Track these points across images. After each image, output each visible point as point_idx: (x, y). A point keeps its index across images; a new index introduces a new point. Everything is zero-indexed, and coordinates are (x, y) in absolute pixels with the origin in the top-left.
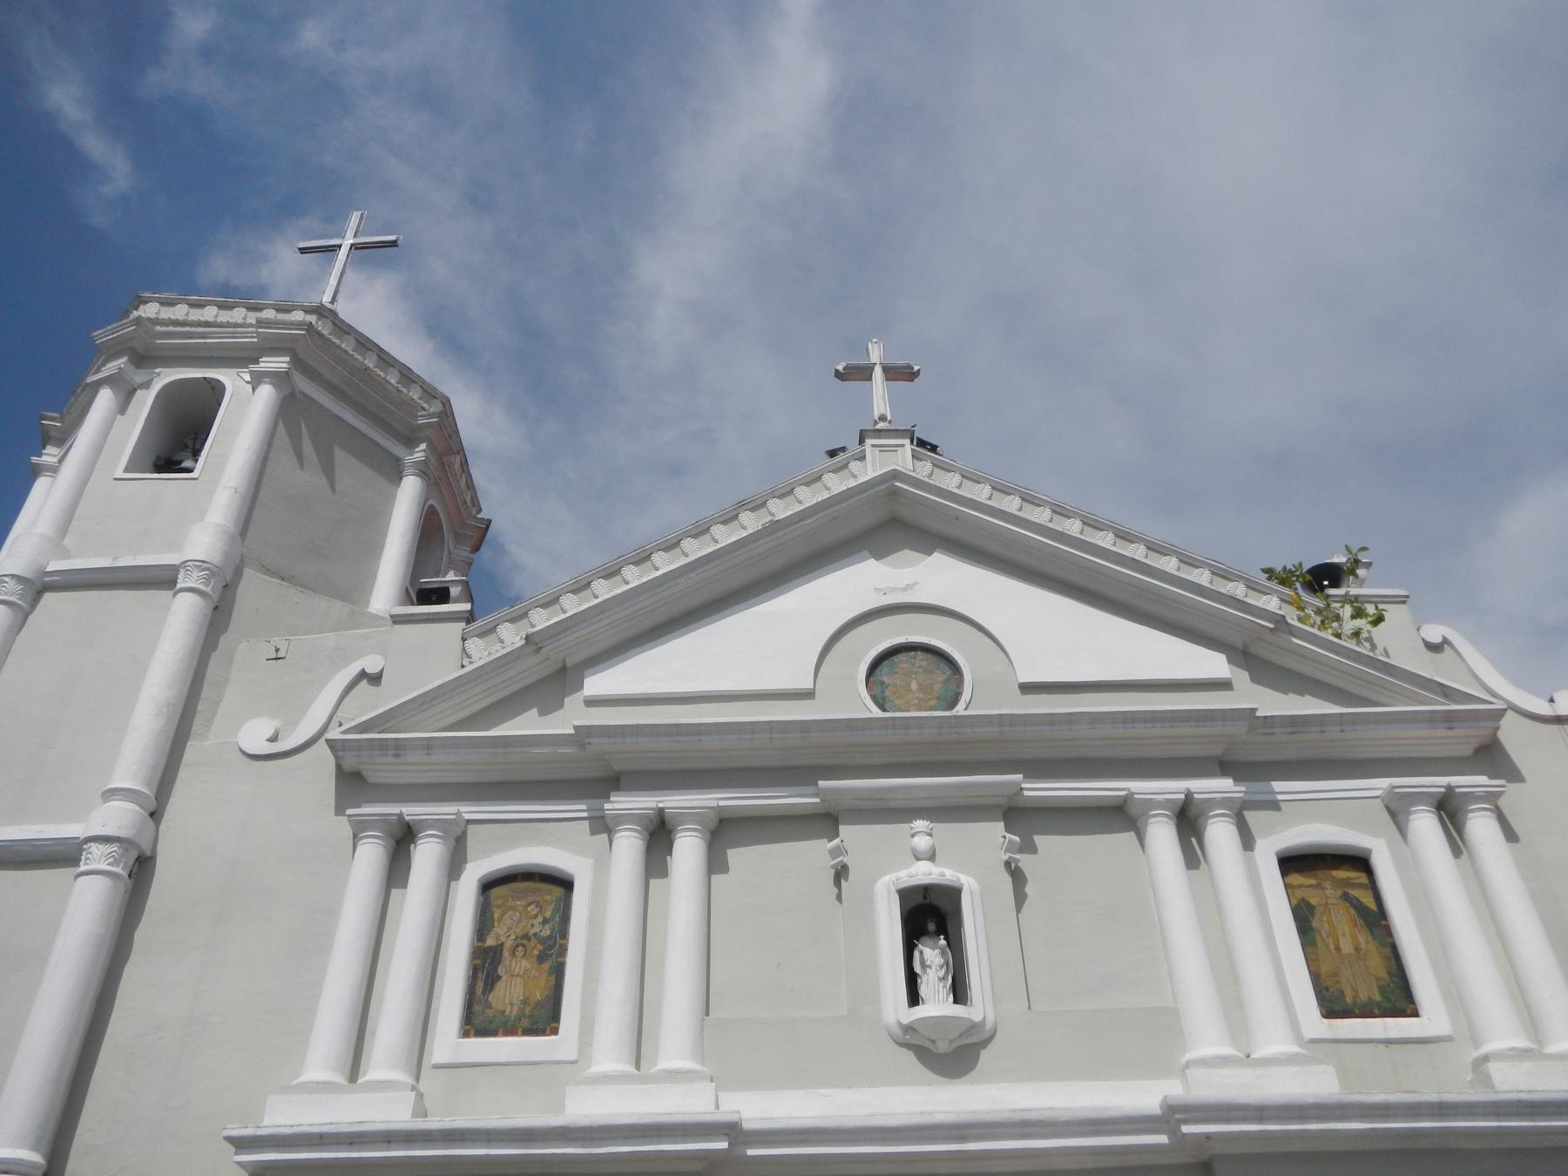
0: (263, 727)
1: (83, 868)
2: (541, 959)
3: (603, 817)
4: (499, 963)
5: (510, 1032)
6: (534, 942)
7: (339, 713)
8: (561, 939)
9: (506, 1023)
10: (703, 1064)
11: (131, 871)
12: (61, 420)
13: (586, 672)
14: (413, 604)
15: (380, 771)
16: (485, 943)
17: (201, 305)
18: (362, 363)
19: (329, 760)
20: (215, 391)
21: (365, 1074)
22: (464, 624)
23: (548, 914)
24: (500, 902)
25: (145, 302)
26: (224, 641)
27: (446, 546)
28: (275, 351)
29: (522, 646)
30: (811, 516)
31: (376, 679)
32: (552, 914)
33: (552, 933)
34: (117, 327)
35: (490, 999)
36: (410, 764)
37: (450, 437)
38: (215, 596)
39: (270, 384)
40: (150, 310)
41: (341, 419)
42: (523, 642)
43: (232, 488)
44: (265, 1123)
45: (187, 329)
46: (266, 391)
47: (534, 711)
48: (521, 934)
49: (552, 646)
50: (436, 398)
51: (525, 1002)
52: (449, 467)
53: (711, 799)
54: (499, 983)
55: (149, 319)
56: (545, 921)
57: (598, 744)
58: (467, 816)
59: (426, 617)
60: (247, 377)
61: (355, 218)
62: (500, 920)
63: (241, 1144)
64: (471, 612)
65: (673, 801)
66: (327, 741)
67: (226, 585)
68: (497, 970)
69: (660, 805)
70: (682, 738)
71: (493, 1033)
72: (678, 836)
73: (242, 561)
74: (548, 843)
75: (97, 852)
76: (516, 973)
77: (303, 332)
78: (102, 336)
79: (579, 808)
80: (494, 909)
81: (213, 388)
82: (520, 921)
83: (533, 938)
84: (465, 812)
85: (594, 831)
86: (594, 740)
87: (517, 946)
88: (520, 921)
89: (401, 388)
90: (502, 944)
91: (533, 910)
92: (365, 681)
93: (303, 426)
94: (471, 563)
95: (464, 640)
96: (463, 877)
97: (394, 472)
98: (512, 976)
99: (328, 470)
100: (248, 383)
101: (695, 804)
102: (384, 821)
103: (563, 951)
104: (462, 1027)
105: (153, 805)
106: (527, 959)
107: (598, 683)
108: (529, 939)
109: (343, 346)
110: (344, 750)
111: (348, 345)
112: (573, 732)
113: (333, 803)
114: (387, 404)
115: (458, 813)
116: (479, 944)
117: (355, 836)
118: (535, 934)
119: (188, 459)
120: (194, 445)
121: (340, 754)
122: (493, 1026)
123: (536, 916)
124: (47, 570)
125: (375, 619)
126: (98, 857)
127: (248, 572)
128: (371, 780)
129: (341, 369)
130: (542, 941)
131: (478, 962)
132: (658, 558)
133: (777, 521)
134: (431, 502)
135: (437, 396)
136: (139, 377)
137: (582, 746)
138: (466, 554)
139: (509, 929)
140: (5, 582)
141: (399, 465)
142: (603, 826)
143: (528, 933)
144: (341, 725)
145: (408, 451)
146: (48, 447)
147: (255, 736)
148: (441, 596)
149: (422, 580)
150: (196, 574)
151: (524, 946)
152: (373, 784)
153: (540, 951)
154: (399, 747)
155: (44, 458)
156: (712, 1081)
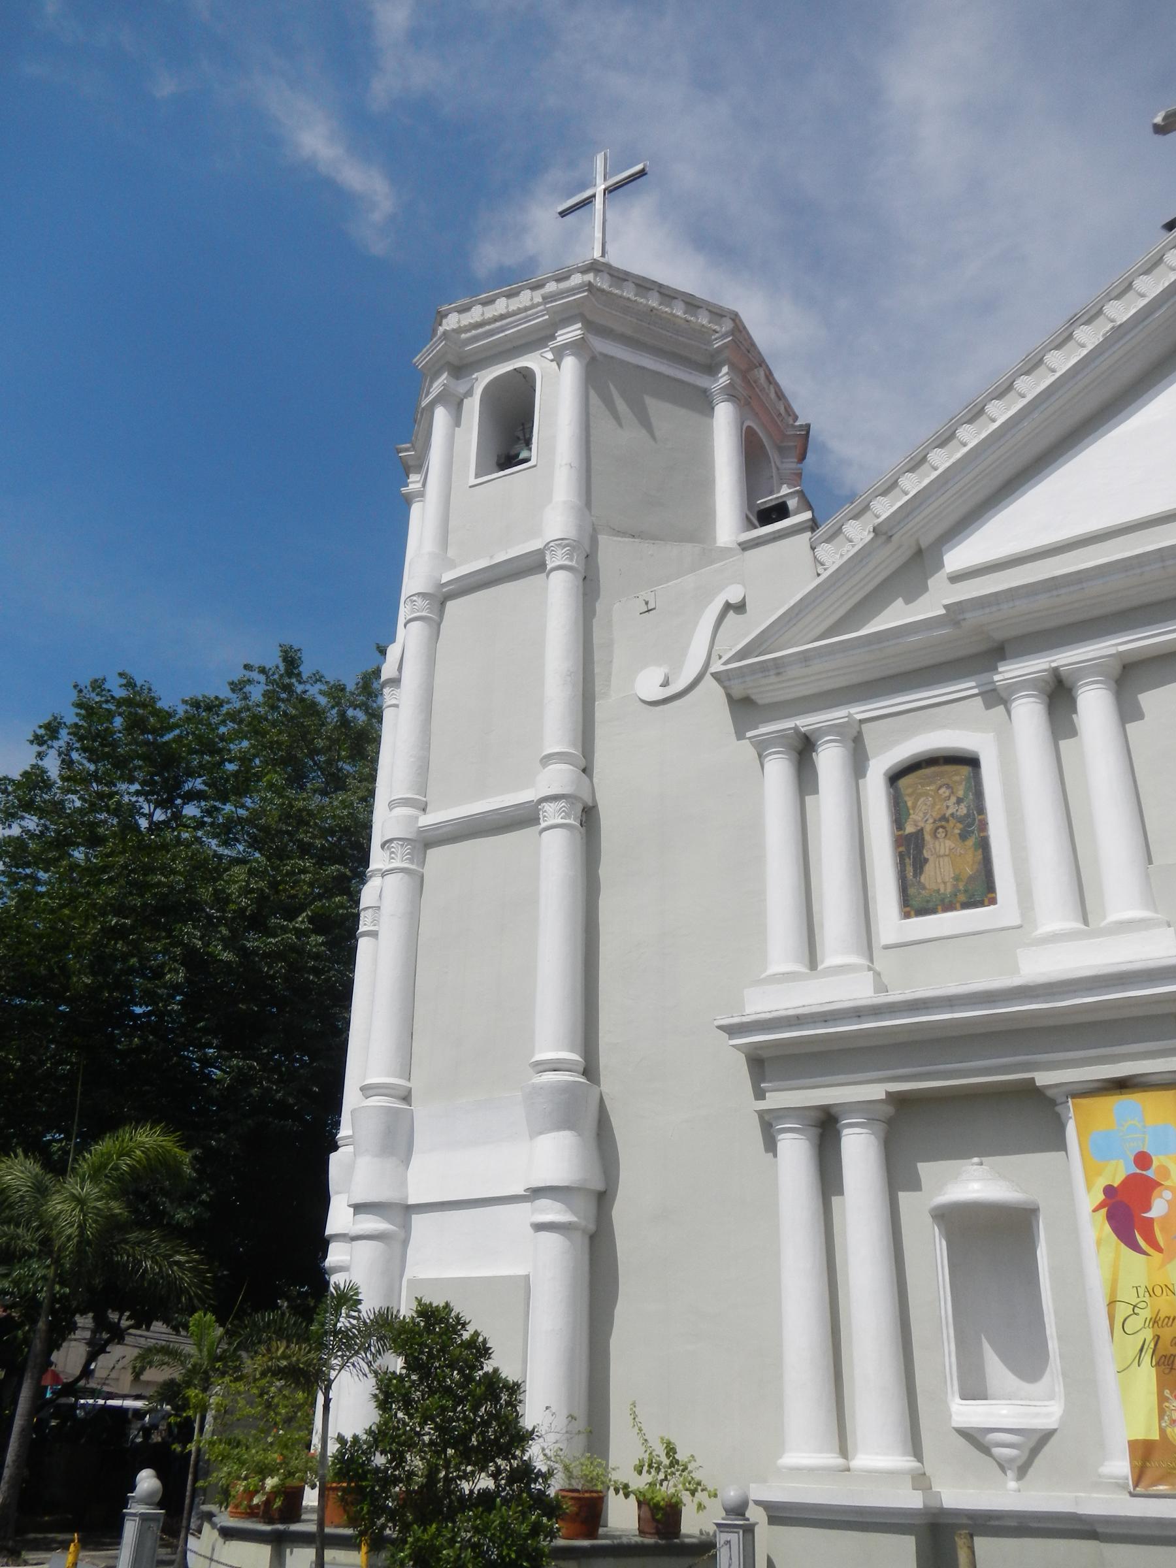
1: (543, 825)
2: (963, 836)
3: (994, 690)
4: (923, 847)
5: (949, 907)
6: (952, 822)
7: (716, 648)
9: (942, 900)
10: (1156, 912)
11: (581, 821)
12: (413, 448)
13: (944, 549)
14: (756, 528)
15: (767, 691)
16: (905, 829)
18: (646, 305)
19: (719, 692)
20: (526, 378)
21: (822, 962)
22: (809, 533)
23: (961, 794)
24: (910, 790)
25: (446, 316)
26: (600, 606)
27: (773, 465)
28: (566, 321)
30: (1160, 307)
31: (740, 608)
32: (965, 793)
33: (968, 810)
34: (431, 347)
35: (922, 879)
36: (795, 679)
37: (749, 352)
38: (581, 568)
39: (572, 355)
40: (451, 322)
41: (644, 368)
42: (872, 535)
43: (566, 464)
44: (747, 1012)
45: (488, 328)
46: (570, 363)
47: (900, 601)
48: (939, 816)
49: (902, 531)
50: (725, 316)
51: (957, 879)
52: (755, 382)
53: (1110, 646)
54: (927, 865)
55: (453, 330)
56: (959, 801)
57: (973, 618)
58: (859, 717)
59: (772, 536)
60: (550, 356)
62: (914, 808)
63: (732, 1030)
64: (813, 520)
65: (1066, 658)
66: (712, 674)
68: (923, 853)
69: (1054, 665)
71: (933, 911)
72: (1079, 692)
73: (594, 530)
74: (943, 727)
76: (942, 852)
77: (586, 294)
78: (421, 360)
79: (968, 686)
80: (907, 798)
81: (524, 377)
82: (933, 805)
83: (951, 818)
84: (857, 713)
85: (988, 706)
86: (968, 615)
87: (937, 828)
88: (933, 805)
90: (922, 830)
91: (944, 793)
92: (731, 612)
93: (611, 385)
94: (801, 474)
95: (813, 548)
96: (869, 774)
97: (704, 403)
98: (939, 856)
99: (645, 422)
100: (552, 361)
101: (1090, 656)
102: (783, 736)
103: (984, 826)
104: (901, 910)
105: (582, 763)
106: (949, 839)
107: (957, 558)
108: (947, 821)
109: (625, 294)
110: (729, 680)
111: (629, 292)
112: (943, 612)
113: (731, 729)
114: (680, 338)
115: (849, 716)
116: (900, 833)
117: (760, 756)
118: (952, 815)
119: (522, 449)
120: (524, 436)
121: (727, 684)
122: (931, 905)
123: (949, 797)
124: (443, 582)
125: (725, 552)
126: (552, 814)
127: (603, 539)
128: (760, 702)
129: (629, 318)
130: (960, 820)
131: (901, 849)
132: (993, 408)
133: (1121, 325)
134: (747, 423)
135: (724, 314)
136: (461, 388)
137: (957, 623)
138: (794, 466)
139: (925, 814)
140: (415, 601)
141: (707, 397)
142: (996, 698)
143: (945, 814)
144: (720, 657)
145: (712, 379)
146: (411, 475)
147: (649, 684)
148: (779, 511)
149: (759, 502)
150: (560, 552)
151: (942, 827)
152: (764, 705)
153: (961, 830)
155: (411, 486)
156: (1169, 926)
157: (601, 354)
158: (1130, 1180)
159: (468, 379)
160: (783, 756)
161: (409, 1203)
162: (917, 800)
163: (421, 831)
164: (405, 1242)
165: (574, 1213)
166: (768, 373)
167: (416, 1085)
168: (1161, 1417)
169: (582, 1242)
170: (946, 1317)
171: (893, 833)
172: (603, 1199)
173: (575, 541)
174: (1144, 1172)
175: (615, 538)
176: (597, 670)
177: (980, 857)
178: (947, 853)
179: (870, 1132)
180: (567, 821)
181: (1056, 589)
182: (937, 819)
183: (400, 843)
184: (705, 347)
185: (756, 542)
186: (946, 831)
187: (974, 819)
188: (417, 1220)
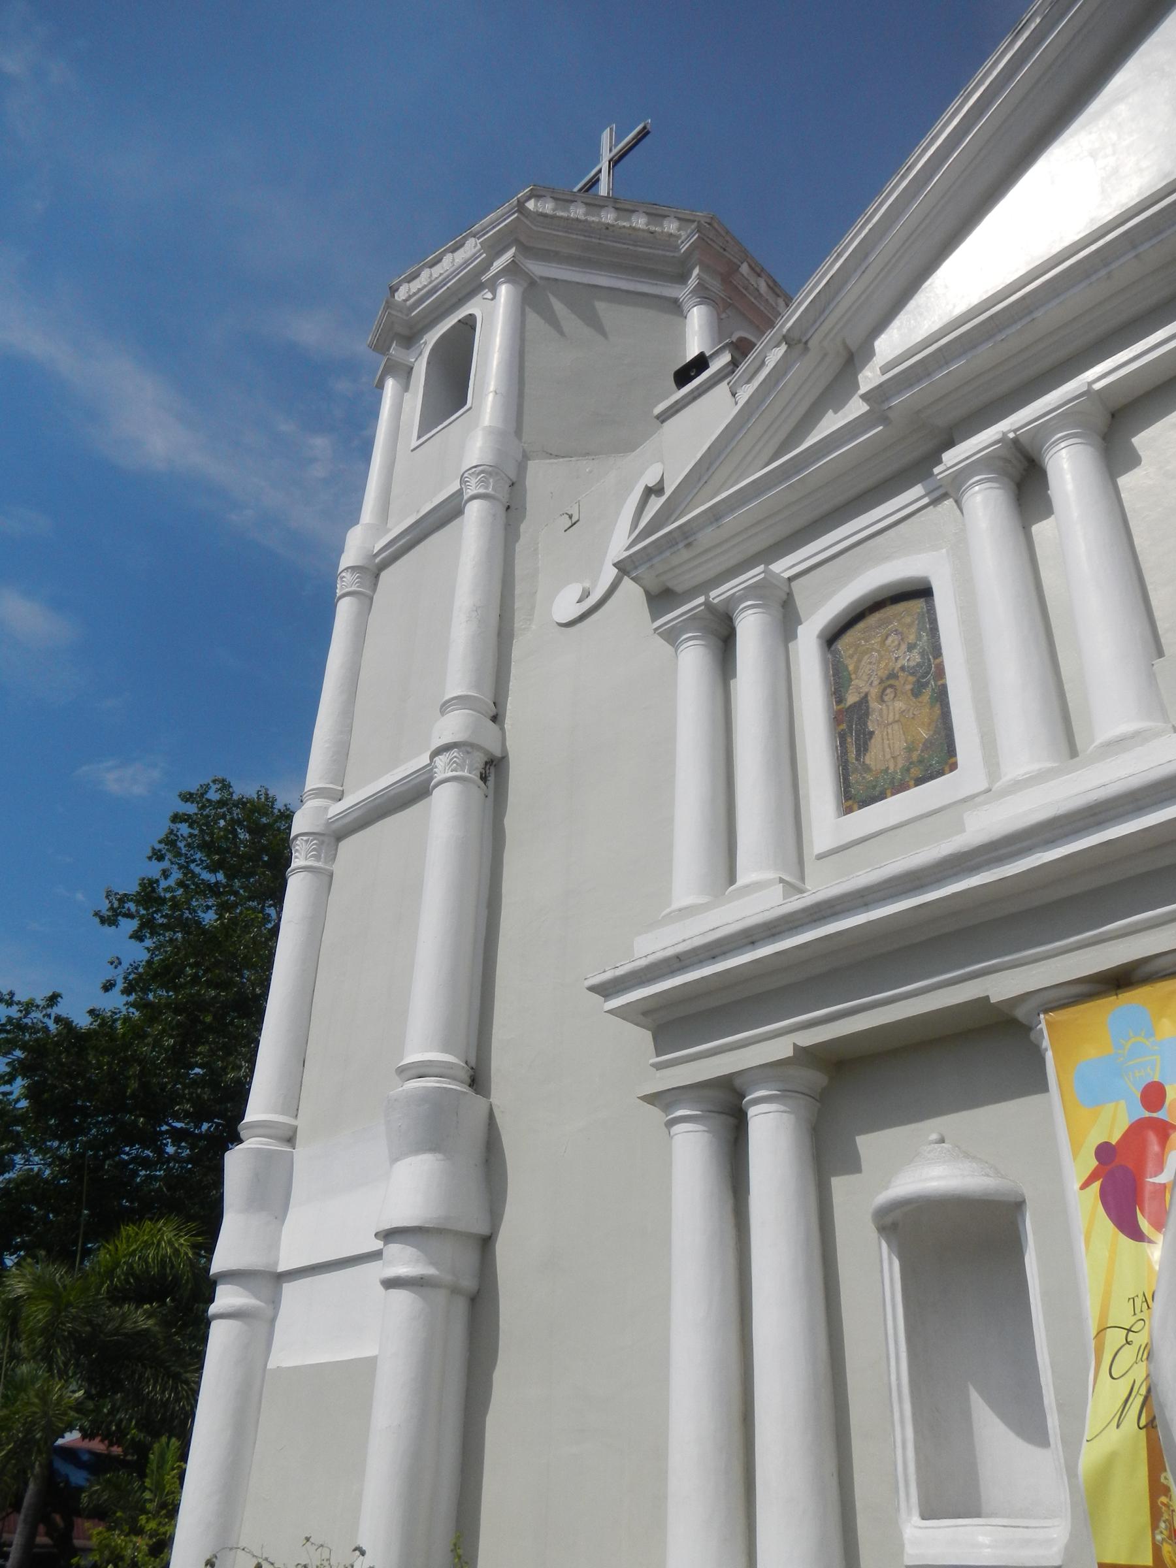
0: (573, 591)
2: (916, 692)
5: (901, 787)
8: (935, 658)
9: (892, 782)
16: (845, 704)
17: (438, 261)
18: (599, 223)
23: (912, 638)
29: (786, 352)
35: (868, 762)
37: (725, 250)
40: (401, 295)
51: (910, 749)
58: (786, 575)
61: (606, 136)
62: (857, 668)
63: (606, 990)
67: (513, 484)
68: (865, 724)
70: (1009, 331)
71: (882, 796)
72: (1046, 460)
75: (441, 763)
76: (890, 720)
77: (516, 215)
87: (885, 689)
89: (652, 228)
90: (866, 695)
91: (893, 642)
92: (653, 496)
95: (734, 395)
98: (888, 724)
102: (693, 618)
103: (941, 672)
105: (492, 711)
110: (636, 568)
116: (839, 707)
118: (903, 668)
123: (899, 644)
128: (679, 589)
131: (844, 726)
139: (870, 676)
141: (679, 306)
143: (893, 670)
147: (566, 605)
151: (891, 686)
152: (684, 593)
154: (686, 534)
157: (541, 278)
158: (1137, 1130)
159: (418, 345)
160: (703, 643)
161: (279, 1271)
162: (859, 661)
163: (329, 823)
164: (273, 1320)
165: (434, 1264)
166: (771, 284)
167: (301, 1123)
168: (1155, 1526)
169: (460, 1307)
170: (899, 1386)
171: (830, 706)
172: (486, 1243)
173: (490, 466)
174: (1155, 1115)
175: (548, 461)
176: (518, 604)
177: (937, 711)
178: (896, 719)
179: (782, 1108)
180: (454, 774)
181: (1000, 331)
182: (884, 676)
183: (305, 838)
184: (672, 254)
185: (674, 409)
186: (896, 693)
187: (930, 665)
188: (288, 1288)
